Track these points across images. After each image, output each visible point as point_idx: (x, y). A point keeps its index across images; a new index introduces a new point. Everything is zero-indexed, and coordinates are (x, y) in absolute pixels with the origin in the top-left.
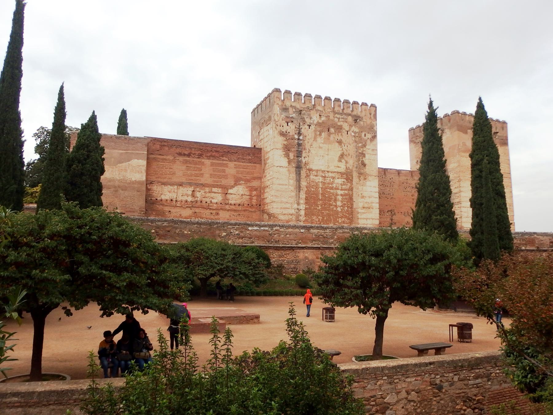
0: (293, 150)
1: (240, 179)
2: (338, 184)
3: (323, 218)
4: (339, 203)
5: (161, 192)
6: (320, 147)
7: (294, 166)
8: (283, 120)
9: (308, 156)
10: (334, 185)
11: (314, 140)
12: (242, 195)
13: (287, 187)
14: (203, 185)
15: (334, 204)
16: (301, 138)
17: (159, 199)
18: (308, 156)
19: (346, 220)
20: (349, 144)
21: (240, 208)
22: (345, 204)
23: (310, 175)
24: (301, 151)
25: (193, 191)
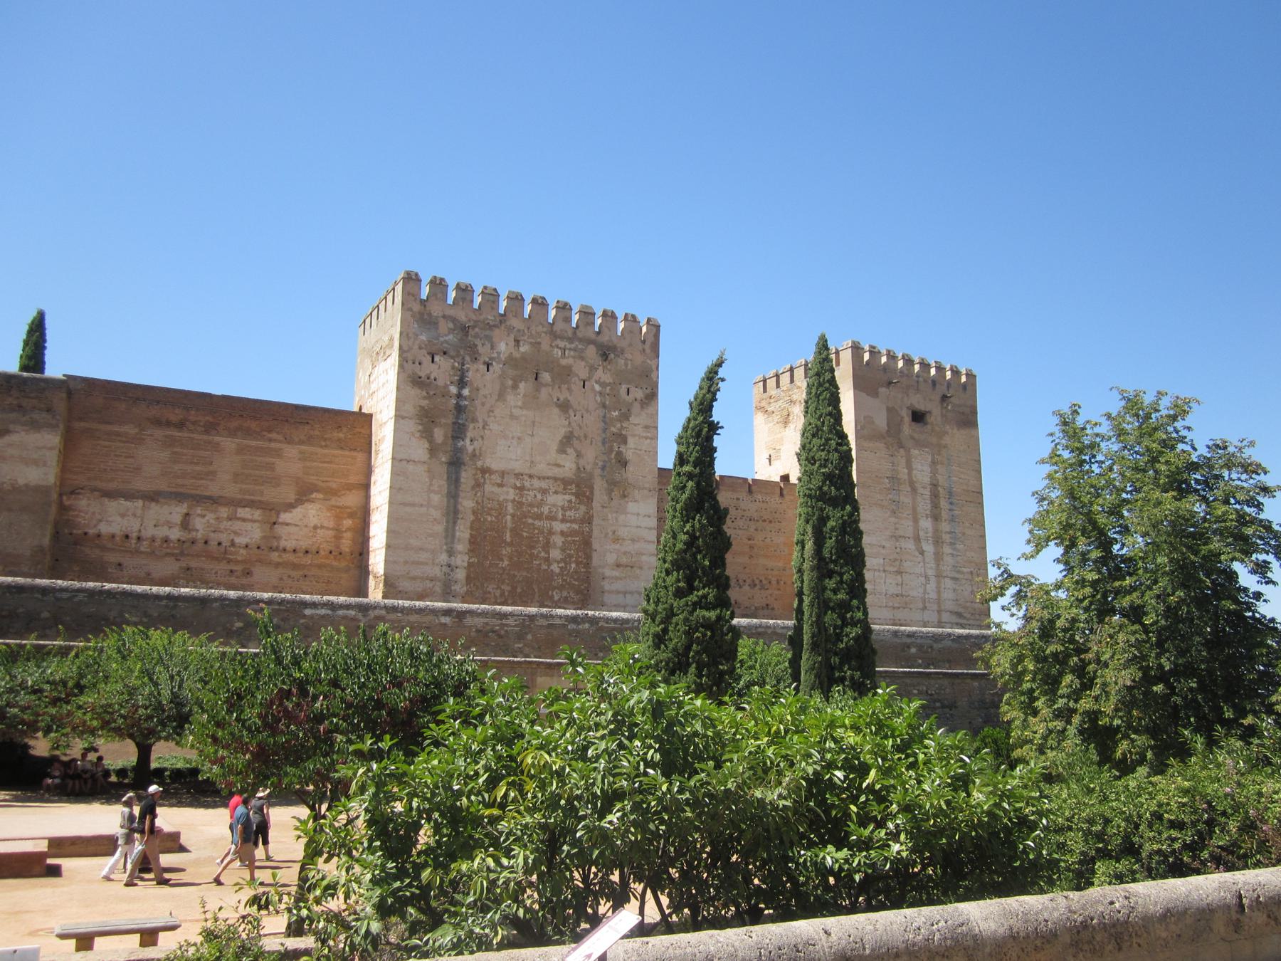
0: (443, 421)
1: (315, 488)
2: (554, 505)
3: (514, 588)
4: (556, 554)
5: (99, 517)
6: (512, 417)
7: (443, 459)
8: (420, 348)
9: (482, 437)
10: (545, 510)
11: (497, 400)
12: (315, 527)
13: (424, 510)
14: (215, 501)
15: (543, 554)
16: (466, 392)
17: (92, 531)
18: (482, 437)
19: (572, 594)
20: (587, 411)
21: (308, 560)
22: (570, 556)
23: (484, 483)
24: (464, 425)
25: (187, 514)
